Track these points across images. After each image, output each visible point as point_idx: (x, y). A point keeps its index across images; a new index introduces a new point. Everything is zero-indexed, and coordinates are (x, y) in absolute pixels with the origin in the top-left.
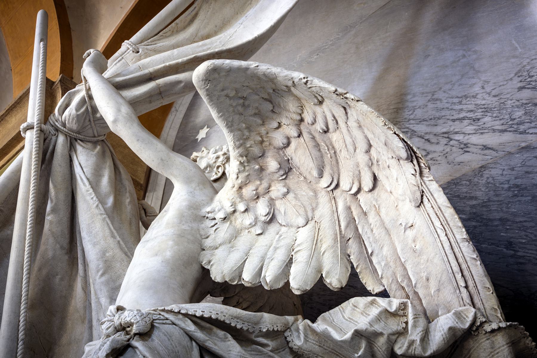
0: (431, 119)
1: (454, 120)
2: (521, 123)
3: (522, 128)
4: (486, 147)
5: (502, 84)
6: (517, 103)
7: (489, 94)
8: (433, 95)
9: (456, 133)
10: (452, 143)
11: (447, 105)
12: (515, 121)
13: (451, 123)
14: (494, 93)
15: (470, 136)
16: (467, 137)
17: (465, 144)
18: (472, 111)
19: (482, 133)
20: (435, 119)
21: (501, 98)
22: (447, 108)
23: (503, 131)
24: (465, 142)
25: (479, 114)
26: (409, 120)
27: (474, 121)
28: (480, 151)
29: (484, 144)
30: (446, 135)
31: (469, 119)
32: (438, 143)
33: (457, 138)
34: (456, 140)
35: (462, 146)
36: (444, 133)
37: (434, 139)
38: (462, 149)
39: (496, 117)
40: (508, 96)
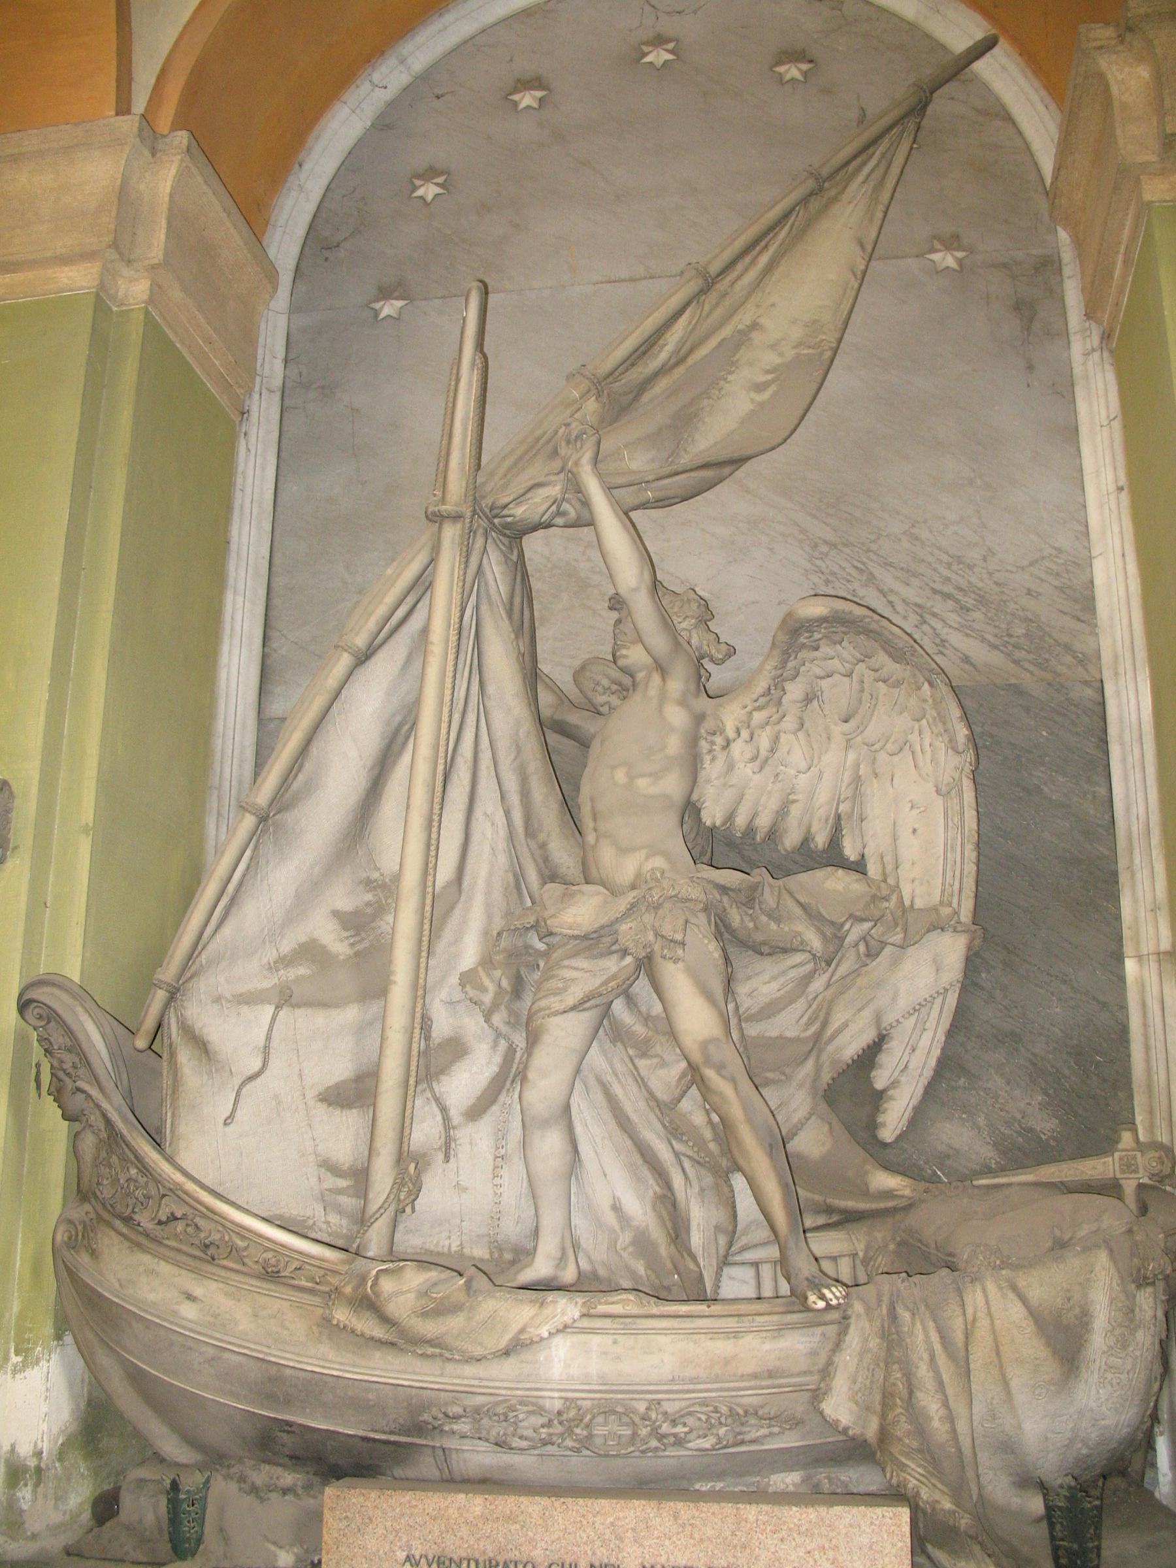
0: (902, 569)
1: (935, 591)
2: (1017, 647)
3: (1018, 655)
4: (966, 659)
5: (1009, 568)
6: (1021, 613)
7: (990, 574)
8: (913, 526)
9: (935, 615)
10: (925, 628)
11: (930, 559)
12: (1012, 641)
13: (929, 593)
14: (996, 576)
15: (951, 631)
16: (946, 630)
17: (943, 641)
18: (961, 590)
19: (967, 635)
20: (908, 571)
21: (1002, 592)
22: (930, 564)
23: (995, 647)
24: (944, 637)
25: (969, 601)
26: (869, 550)
27: (961, 608)
28: (958, 662)
29: (967, 653)
30: (919, 611)
31: (957, 601)
32: (905, 618)
33: (933, 624)
34: (932, 627)
35: (938, 641)
36: (916, 605)
37: (900, 607)
38: (937, 645)
39: (990, 619)
40: (1013, 594)
